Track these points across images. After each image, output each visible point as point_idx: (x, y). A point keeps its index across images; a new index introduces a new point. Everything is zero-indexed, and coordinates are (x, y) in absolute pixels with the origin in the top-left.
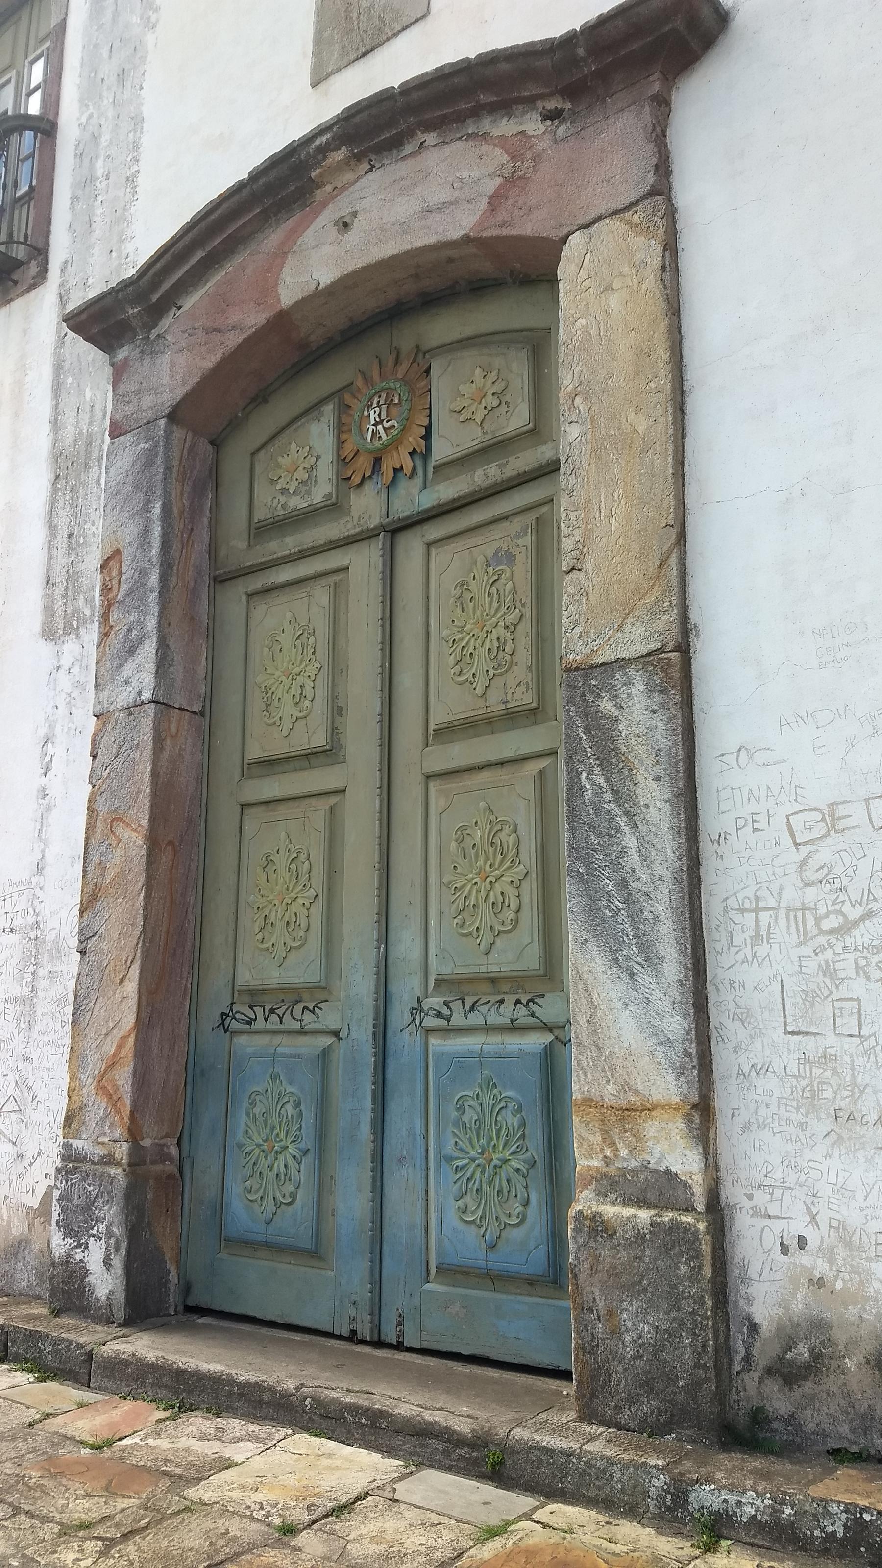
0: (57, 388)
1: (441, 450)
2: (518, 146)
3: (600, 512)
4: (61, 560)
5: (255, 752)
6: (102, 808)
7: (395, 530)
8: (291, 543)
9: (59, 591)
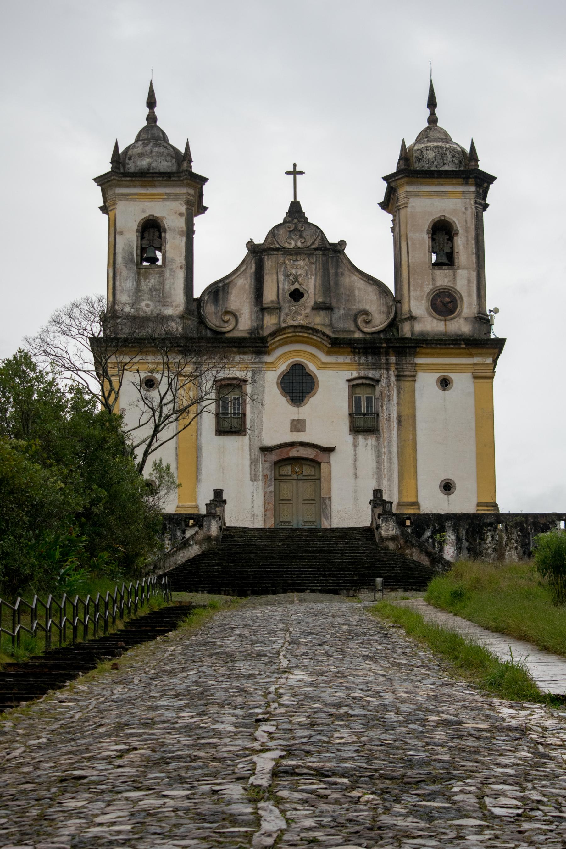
1: (304, 474)
2: (317, 452)
3: (324, 485)
4: (253, 472)
8: (284, 478)
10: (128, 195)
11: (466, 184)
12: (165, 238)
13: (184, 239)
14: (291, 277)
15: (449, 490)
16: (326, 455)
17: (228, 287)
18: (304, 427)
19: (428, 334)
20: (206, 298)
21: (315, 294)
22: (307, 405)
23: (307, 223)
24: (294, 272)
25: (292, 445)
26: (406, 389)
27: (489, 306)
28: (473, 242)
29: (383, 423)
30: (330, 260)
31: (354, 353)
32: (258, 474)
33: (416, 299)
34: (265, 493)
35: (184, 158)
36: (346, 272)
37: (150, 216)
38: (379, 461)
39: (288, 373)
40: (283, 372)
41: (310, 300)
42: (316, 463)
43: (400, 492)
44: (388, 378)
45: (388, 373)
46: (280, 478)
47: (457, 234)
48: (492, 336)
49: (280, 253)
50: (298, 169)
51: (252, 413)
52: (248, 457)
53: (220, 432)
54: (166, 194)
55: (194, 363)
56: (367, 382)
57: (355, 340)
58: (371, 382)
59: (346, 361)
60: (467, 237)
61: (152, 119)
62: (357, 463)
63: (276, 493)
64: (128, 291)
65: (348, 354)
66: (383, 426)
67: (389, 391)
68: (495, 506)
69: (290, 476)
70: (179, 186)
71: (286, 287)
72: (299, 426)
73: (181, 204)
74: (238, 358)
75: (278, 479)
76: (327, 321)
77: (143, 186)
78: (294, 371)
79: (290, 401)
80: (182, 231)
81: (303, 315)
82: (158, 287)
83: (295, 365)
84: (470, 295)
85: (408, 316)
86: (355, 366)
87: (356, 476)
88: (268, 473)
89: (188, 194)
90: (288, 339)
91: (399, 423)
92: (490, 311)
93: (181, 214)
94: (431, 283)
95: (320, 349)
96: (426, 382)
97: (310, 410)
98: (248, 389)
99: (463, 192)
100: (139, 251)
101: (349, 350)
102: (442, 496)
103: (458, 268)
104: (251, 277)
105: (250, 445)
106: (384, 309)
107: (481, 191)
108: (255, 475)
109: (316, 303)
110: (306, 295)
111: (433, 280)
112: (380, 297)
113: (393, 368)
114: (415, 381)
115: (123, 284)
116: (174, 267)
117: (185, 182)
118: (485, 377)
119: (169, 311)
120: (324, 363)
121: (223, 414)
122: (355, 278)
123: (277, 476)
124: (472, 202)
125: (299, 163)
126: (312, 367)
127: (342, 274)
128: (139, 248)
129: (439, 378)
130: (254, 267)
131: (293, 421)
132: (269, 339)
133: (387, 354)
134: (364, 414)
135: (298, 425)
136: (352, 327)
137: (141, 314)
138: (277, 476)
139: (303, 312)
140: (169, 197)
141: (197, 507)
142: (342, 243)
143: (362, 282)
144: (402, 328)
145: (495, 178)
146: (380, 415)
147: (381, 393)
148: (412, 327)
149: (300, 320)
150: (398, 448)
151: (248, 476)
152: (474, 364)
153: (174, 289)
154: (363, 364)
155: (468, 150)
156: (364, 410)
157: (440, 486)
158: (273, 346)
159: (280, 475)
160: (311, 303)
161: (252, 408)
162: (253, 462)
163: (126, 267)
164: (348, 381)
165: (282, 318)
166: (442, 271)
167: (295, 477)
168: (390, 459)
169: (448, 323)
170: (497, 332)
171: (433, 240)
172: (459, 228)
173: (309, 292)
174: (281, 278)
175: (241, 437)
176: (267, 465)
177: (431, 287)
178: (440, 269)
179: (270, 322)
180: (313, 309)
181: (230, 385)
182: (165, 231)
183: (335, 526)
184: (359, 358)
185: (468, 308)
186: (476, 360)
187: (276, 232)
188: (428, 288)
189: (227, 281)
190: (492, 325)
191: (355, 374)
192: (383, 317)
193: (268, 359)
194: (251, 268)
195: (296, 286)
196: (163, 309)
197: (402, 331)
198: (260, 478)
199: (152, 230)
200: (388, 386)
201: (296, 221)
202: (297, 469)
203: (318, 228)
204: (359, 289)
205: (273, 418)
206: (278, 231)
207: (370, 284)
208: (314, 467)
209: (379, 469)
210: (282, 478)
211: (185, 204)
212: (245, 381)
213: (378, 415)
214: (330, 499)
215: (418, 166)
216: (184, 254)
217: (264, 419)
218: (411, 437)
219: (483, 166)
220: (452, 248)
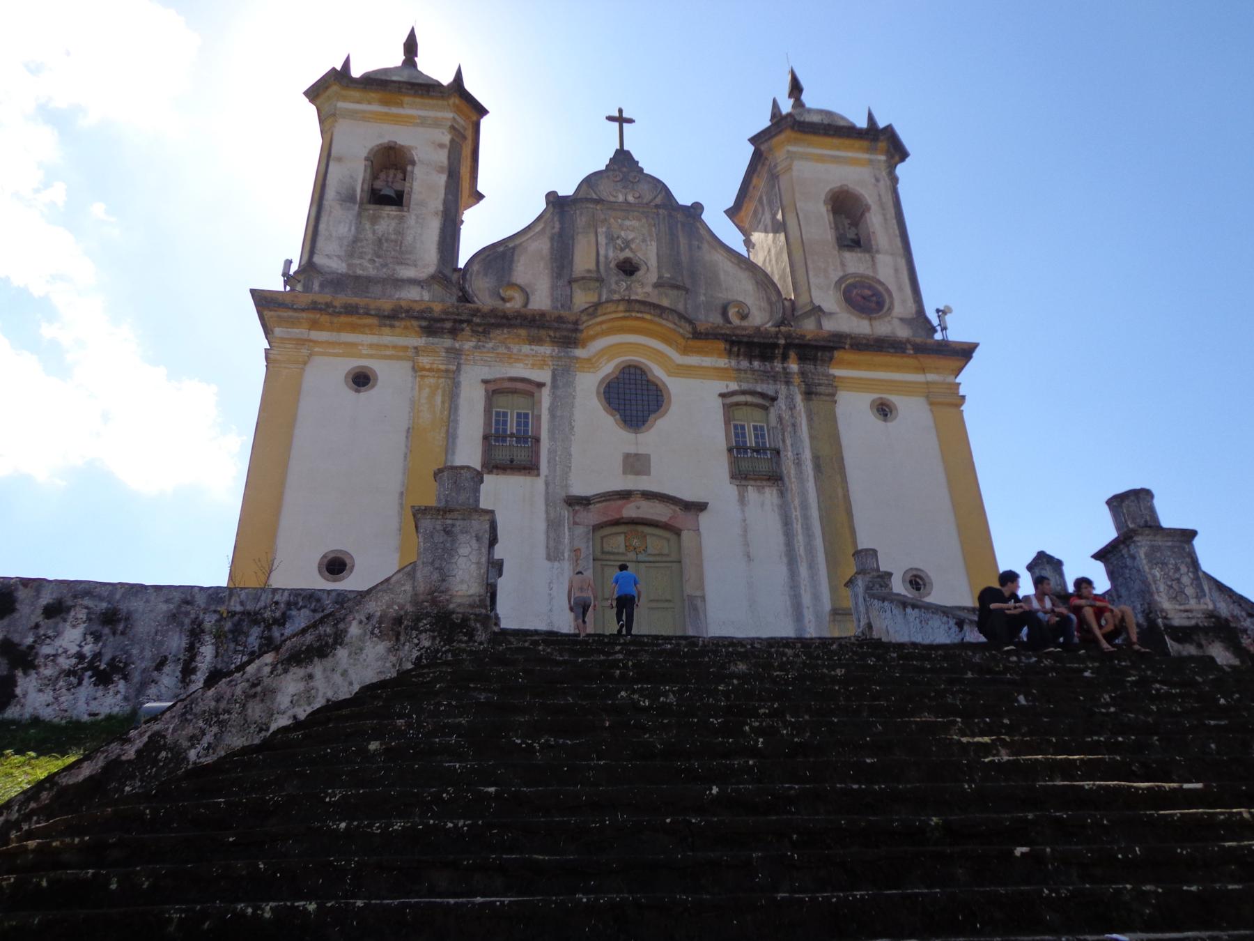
0: (547, 505)
1: (649, 551)
2: (674, 511)
4: (552, 544)
10: (356, 112)
11: (872, 150)
12: (412, 172)
13: (443, 178)
17: (513, 254)
20: (475, 267)
21: (659, 267)
22: (653, 430)
24: (623, 234)
25: (626, 495)
28: (894, 221)
29: (788, 468)
31: (730, 353)
36: (705, 246)
40: (608, 375)
41: (649, 276)
44: (790, 398)
46: (604, 557)
50: (625, 115)
51: (552, 438)
52: (542, 515)
54: (420, 117)
60: (884, 215)
64: (340, 239)
65: (720, 356)
66: (789, 473)
67: (792, 416)
71: (611, 254)
74: (526, 349)
77: (385, 103)
78: (627, 376)
81: (644, 287)
83: (630, 366)
84: (900, 289)
85: (809, 308)
87: (749, 557)
88: (582, 546)
91: (818, 468)
92: (938, 311)
93: (441, 146)
97: (657, 438)
98: (545, 396)
103: (878, 252)
104: (552, 239)
105: (547, 493)
106: (764, 304)
109: (660, 277)
111: (843, 265)
113: (797, 380)
117: (451, 102)
121: (497, 438)
122: (719, 257)
123: (598, 554)
126: (658, 372)
127: (699, 248)
129: (873, 401)
130: (557, 225)
131: (627, 457)
132: (584, 318)
133: (785, 358)
135: (636, 463)
137: (359, 272)
138: (598, 554)
139: (640, 290)
140: (423, 122)
146: (782, 454)
147: (780, 418)
150: (820, 509)
151: (541, 551)
152: (927, 383)
154: (745, 371)
159: (603, 552)
160: (653, 277)
161: (552, 432)
162: (553, 525)
164: (722, 395)
166: (854, 254)
168: (807, 528)
169: (876, 323)
174: (602, 240)
175: (528, 479)
176: (580, 530)
177: (841, 274)
179: (582, 299)
180: (657, 286)
181: (514, 392)
185: (902, 306)
186: (931, 377)
188: (835, 275)
189: (511, 245)
191: (734, 386)
193: (579, 352)
195: (627, 254)
196: (397, 268)
198: (566, 555)
199: (392, 172)
202: (635, 542)
208: (668, 540)
210: (608, 557)
212: (540, 385)
213: (778, 452)
214: (703, 598)
217: (574, 450)
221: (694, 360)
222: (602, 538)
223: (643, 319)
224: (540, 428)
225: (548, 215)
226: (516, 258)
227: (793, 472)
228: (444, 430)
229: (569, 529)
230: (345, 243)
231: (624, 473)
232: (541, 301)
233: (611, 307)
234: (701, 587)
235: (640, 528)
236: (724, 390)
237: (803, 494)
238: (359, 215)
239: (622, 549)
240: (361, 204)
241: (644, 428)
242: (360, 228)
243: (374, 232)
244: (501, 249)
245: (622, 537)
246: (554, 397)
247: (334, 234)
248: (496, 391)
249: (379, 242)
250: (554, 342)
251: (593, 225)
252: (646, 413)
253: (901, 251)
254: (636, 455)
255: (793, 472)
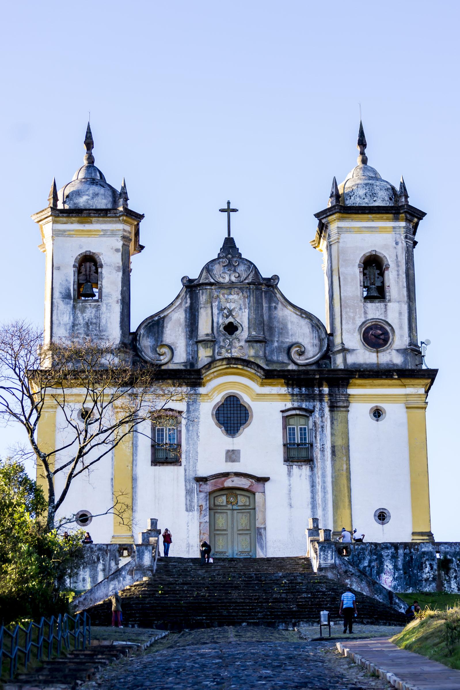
0: (186, 482)
1: (239, 504)
2: (252, 482)
3: (259, 516)
4: (188, 503)
5: (216, 528)
6: (202, 532)
7: (233, 510)
9: (188, 506)
10: (65, 231)
11: (396, 219)
13: (120, 274)
14: (226, 311)
15: (384, 519)
16: (260, 485)
17: (163, 321)
18: (239, 458)
19: (360, 365)
20: (142, 331)
21: (249, 328)
23: (241, 258)
24: (228, 305)
25: (226, 475)
26: (339, 420)
27: (421, 338)
28: (404, 276)
29: (317, 453)
30: (263, 294)
31: (288, 385)
32: (193, 504)
33: (348, 332)
34: (200, 523)
35: (119, 196)
36: (280, 306)
37: (86, 251)
38: (313, 492)
39: (223, 404)
40: (218, 403)
41: (244, 334)
42: (250, 492)
43: (335, 522)
44: (322, 409)
45: (321, 405)
47: (387, 268)
48: (424, 367)
49: (213, 287)
51: (188, 443)
52: (184, 487)
53: (156, 462)
55: (130, 395)
56: (301, 413)
57: (289, 371)
58: (304, 413)
59: (280, 393)
60: (398, 271)
61: (91, 160)
62: (292, 493)
63: (212, 523)
65: (282, 386)
66: (317, 456)
67: (322, 422)
68: (430, 535)
69: (225, 506)
70: (116, 222)
71: (221, 321)
72: (233, 456)
73: (117, 240)
74: (172, 389)
75: (213, 509)
76: (261, 353)
77: (80, 222)
79: (224, 432)
80: (118, 267)
82: (94, 321)
83: (230, 396)
84: (401, 328)
85: (340, 348)
86: (290, 397)
88: (204, 504)
89: (124, 230)
90: (222, 371)
91: (333, 453)
92: (422, 343)
93: (117, 250)
94: (363, 316)
95: (254, 381)
96: (358, 412)
97: (245, 439)
99: (394, 228)
100: (76, 286)
101: (283, 381)
102: (376, 525)
103: (390, 301)
104: (186, 311)
106: (316, 342)
107: (411, 227)
108: (191, 505)
110: (240, 329)
111: (365, 313)
112: (313, 331)
113: (326, 399)
114: (348, 411)
115: (60, 318)
116: (110, 301)
117: (121, 218)
118: (417, 407)
119: (104, 345)
120: (258, 394)
123: (212, 506)
124: (403, 237)
125: (233, 190)
126: (246, 399)
127: (276, 308)
128: (76, 283)
129: (372, 409)
130: (189, 301)
132: (203, 371)
133: (320, 385)
134: (298, 445)
135: (232, 456)
136: (286, 360)
138: (212, 506)
140: (105, 233)
141: (132, 536)
142: (276, 278)
143: (295, 316)
144: (335, 360)
145: (424, 214)
146: (314, 445)
147: (315, 423)
148: (345, 359)
149: (236, 353)
150: (332, 477)
151: (184, 507)
153: (110, 322)
154: (297, 395)
155: (398, 188)
156: (298, 440)
157: (375, 515)
158: (208, 378)
161: (187, 439)
162: (189, 492)
163: (63, 301)
164: (282, 411)
165: (216, 351)
166: (373, 304)
167: (230, 506)
168: (324, 488)
169: (379, 354)
170: (428, 363)
171: (364, 274)
172: (390, 263)
173: (243, 326)
174: (216, 311)
175: (176, 468)
176: (202, 495)
177: (363, 320)
178: (371, 302)
179: (204, 355)
180: (247, 341)
182: (101, 266)
183: (270, 555)
184: (293, 389)
185: (400, 340)
187: (210, 267)
189: (162, 316)
190: (423, 356)
191: (289, 405)
192: (317, 349)
193: (202, 390)
194: (186, 303)
195: (231, 319)
197: (335, 363)
198: (196, 508)
200: (322, 417)
201: (230, 256)
202: (232, 499)
203: (251, 263)
204: (292, 322)
205: (208, 448)
206: (212, 266)
207: (302, 317)
208: (249, 497)
209: (313, 498)
211: (122, 240)
213: (312, 445)
214: (265, 528)
215: (349, 203)
216: (120, 289)
217: (199, 450)
218: (345, 467)
219: (414, 201)
220: (383, 283)
221: (267, 390)
222: (214, 497)
223: (237, 368)
224: (181, 438)
225: (183, 293)
226: (165, 325)
227: (319, 456)
228: (131, 442)
229: (197, 494)
230: (68, 328)
231: (226, 461)
232: (181, 357)
233: (219, 363)
234: (264, 522)
235: (234, 491)
236: (284, 408)
237: (324, 469)
238: (74, 307)
239: (225, 504)
240: (74, 299)
241: (237, 435)
242: (75, 318)
243: (84, 319)
244: (156, 318)
245: (225, 496)
246: (188, 418)
247: (62, 323)
248: (157, 417)
249: (87, 324)
250: (187, 385)
251: (210, 300)
252: (239, 425)
253: (406, 299)
254: (233, 450)
255: (319, 456)
